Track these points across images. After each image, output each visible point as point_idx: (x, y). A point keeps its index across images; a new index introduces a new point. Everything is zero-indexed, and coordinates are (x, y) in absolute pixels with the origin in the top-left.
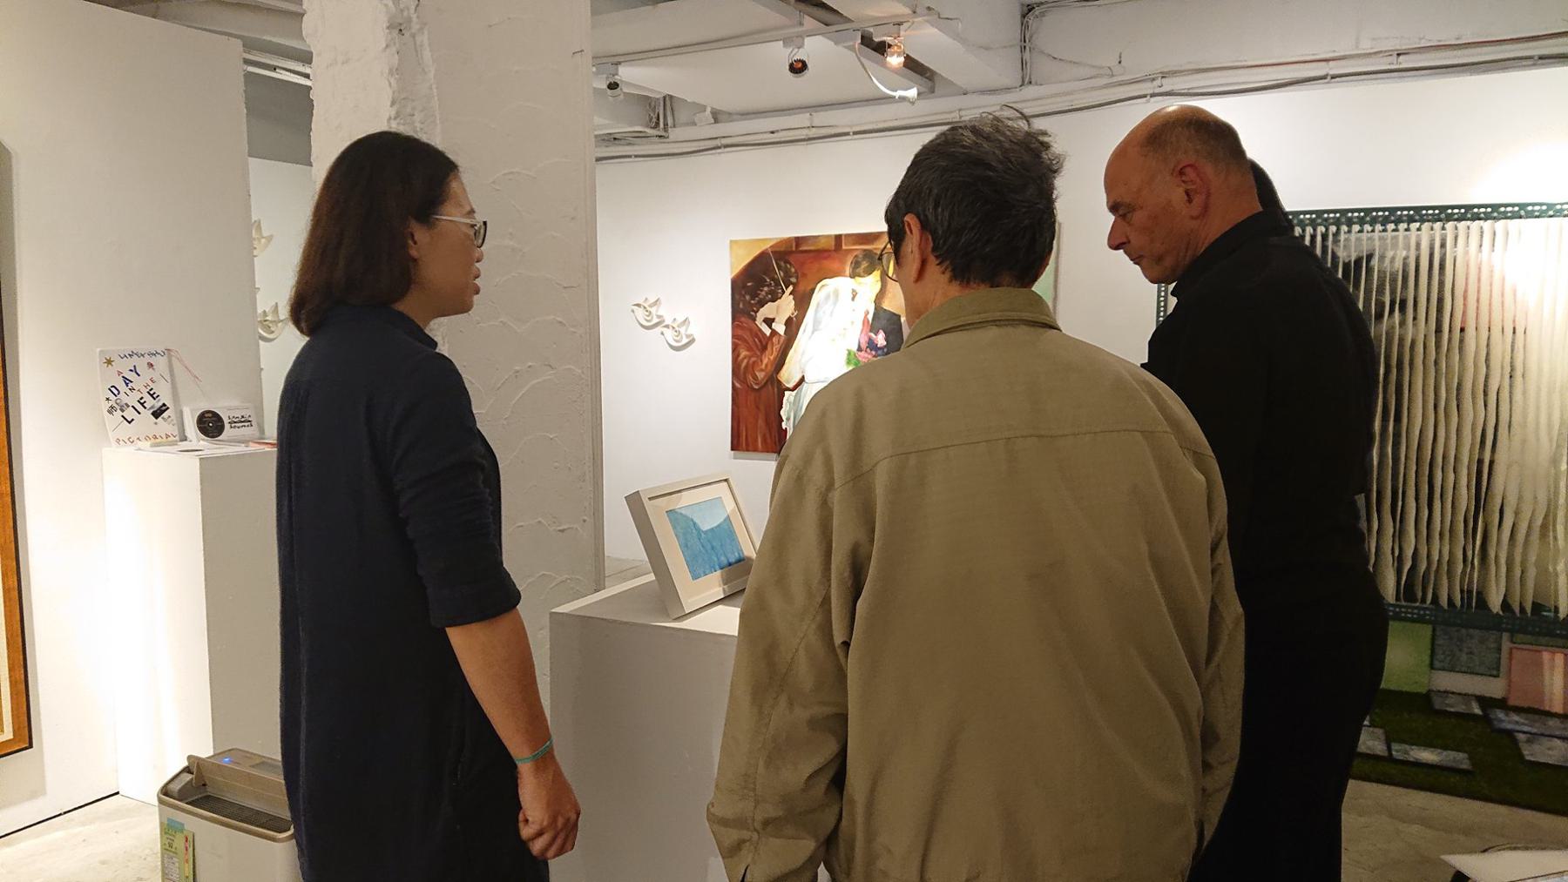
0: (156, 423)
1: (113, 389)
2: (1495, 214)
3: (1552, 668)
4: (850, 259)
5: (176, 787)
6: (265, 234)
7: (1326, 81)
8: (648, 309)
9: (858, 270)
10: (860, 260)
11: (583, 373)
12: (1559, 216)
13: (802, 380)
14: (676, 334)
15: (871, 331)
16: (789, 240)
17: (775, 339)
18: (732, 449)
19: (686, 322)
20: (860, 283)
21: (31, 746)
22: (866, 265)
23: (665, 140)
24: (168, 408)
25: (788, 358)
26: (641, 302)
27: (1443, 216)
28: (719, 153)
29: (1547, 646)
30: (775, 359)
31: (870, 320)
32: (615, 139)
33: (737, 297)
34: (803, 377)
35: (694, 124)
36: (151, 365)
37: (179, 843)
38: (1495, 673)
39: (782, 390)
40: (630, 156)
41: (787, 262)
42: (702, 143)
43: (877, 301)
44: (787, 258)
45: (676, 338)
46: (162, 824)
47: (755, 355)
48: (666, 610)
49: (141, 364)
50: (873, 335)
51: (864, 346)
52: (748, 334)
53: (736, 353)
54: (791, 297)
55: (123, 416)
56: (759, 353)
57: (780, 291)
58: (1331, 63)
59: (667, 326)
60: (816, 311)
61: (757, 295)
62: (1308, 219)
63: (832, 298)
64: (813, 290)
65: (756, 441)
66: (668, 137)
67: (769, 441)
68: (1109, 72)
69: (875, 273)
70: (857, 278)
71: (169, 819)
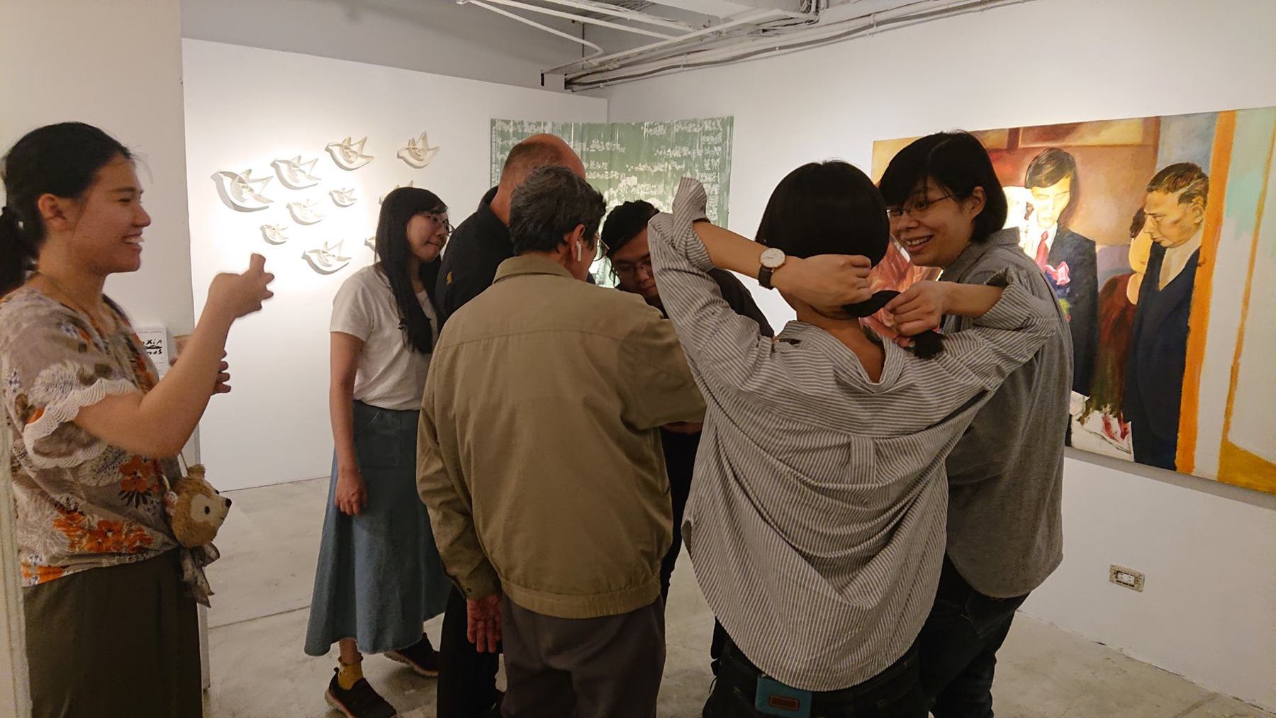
4: (1028, 160)
9: (1038, 177)
15: (1049, 262)
20: (1040, 195)
22: (1051, 169)
31: (1049, 247)
32: (764, 31)
40: (774, 49)
50: (1051, 268)
56: (894, 283)
66: (818, 21)
69: (1061, 181)
70: (1035, 188)
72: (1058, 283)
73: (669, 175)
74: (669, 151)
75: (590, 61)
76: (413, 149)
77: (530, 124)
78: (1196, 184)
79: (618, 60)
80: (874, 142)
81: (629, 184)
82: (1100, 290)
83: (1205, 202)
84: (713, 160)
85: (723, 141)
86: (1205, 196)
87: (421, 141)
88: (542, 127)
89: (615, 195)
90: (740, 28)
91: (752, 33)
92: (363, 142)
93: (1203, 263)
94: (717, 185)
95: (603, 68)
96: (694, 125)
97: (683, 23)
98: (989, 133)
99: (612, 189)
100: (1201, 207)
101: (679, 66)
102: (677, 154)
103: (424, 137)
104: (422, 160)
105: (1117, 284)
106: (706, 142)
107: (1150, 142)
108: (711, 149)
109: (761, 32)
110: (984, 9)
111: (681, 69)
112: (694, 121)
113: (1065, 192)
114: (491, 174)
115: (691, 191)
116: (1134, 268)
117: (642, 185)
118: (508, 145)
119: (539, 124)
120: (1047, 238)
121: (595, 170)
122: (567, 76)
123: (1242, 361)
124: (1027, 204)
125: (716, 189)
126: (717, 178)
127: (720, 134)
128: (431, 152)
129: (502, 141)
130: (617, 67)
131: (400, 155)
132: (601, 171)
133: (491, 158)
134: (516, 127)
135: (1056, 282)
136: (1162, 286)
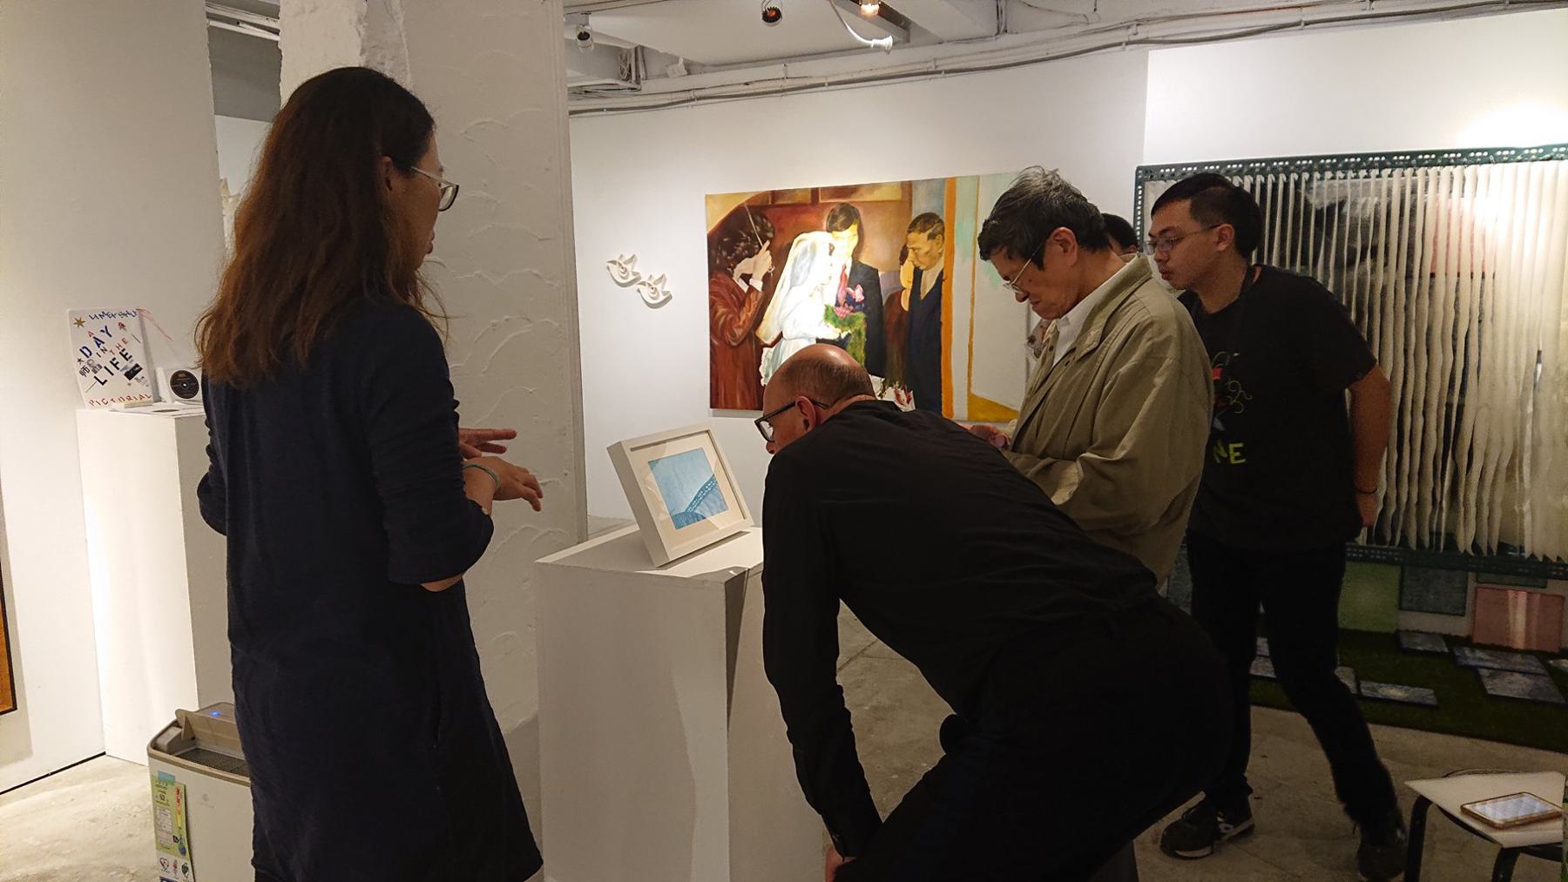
0: (129, 384)
1: (85, 350)
2: (1465, 160)
3: (1515, 607)
4: (826, 214)
5: (164, 742)
7: (1299, 27)
8: (624, 265)
9: (834, 225)
10: (837, 214)
11: (560, 326)
12: (1526, 161)
13: (781, 336)
14: (652, 291)
15: (849, 286)
16: (766, 194)
17: (752, 296)
18: (711, 407)
19: (662, 278)
21: (15, 708)
24: (141, 369)
25: (766, 313)
26: (616, 258)
27: (1414, 161)
28: (692, 106)
29: (1510, 584)
30: (753, 315)
32: (586, 92)
33: (713, 253)
35: (666, 76)
36: (122, 326)
37: (171, 796)
38: (1460, 611)
39: (760, 347)
40: (602, 110)
41: (763, 216)
42: (674, 95)
44: (763, 212)
45: (652, 295)
46: (152, 776)
47: (733, 312)
48: (651, 561)
49: (112, 325)
50: (850, 290)
51: (842, 301)
52: (725, 290)
53: (714, 308)
54: (768, 252)
55: (95, 377)
56: (735, 309)
57: (757, 246)
58: (1304, 9)
59: (643, 284)
60: (794, 266)
61: (734, 251)
62: (1282, 166)
63: (809, 255)
65: (735, 398)
67: (747, 397)
68: (1084, 20)
70: (834, 232)
71: (159, 772)
78: (937, 227)
80: (706, 196)
82: (884, 302)
83: (943, 238)
86: (943, 235)
93: (947, 277)
100: (941, 242)
105: (895, 297)
107: (907, 199)
116: (904, 286)
123: (974, 340)
136: (922, 297)
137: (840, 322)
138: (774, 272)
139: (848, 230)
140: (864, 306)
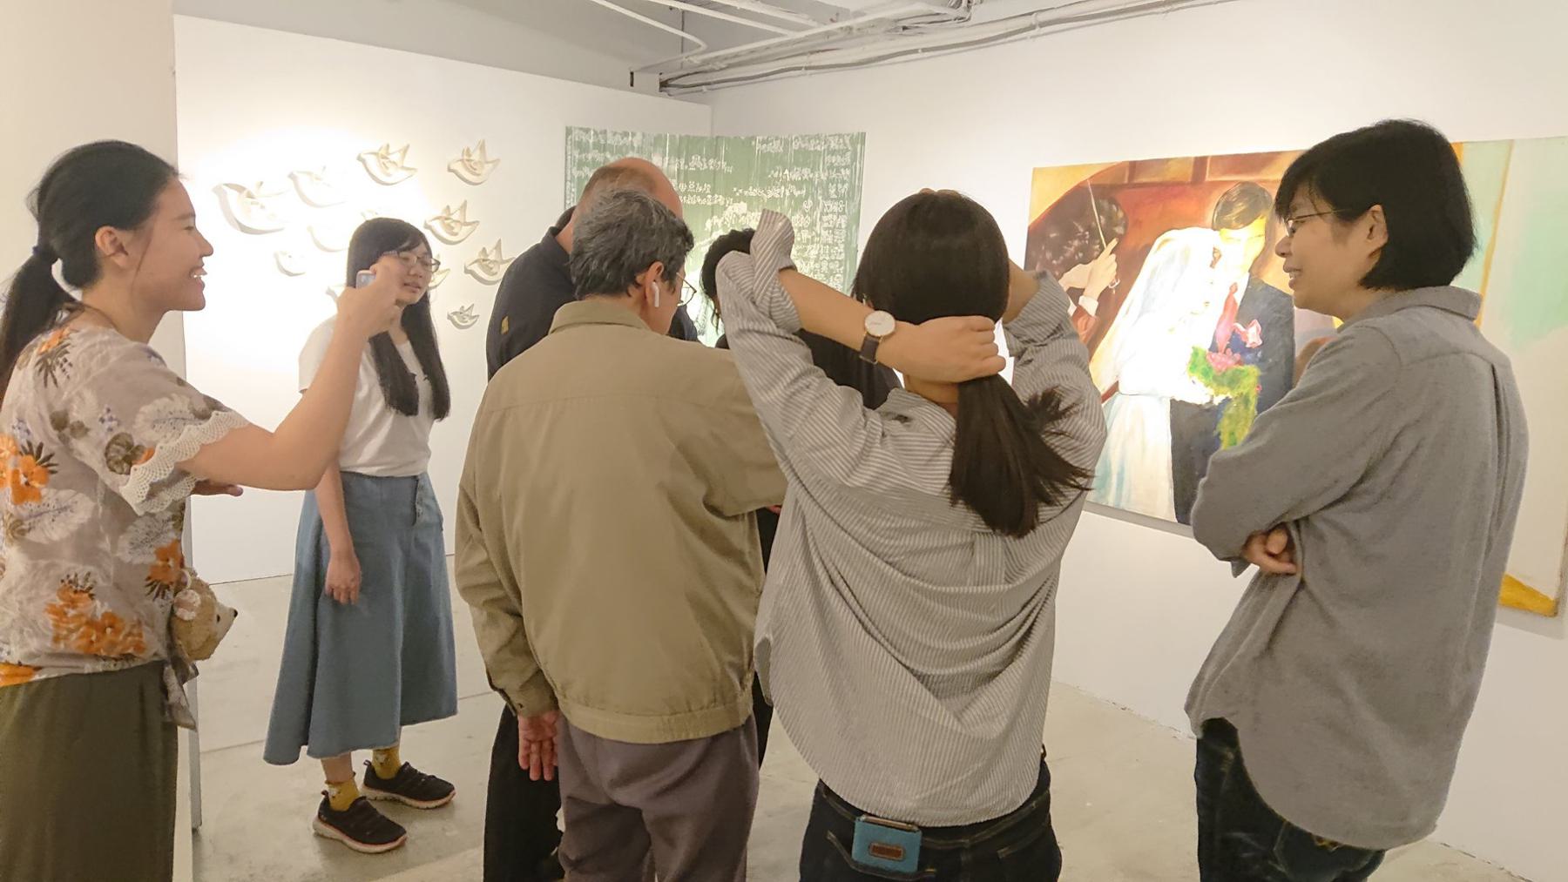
4: (1216, 197)
6: (491, 156)
9: (1227, 217)
13: (1114, 389)
15: (1238, 319)
16: (1118, 168)
17: (1081, 322)
22: (1243, 208)
23: (969, 23)
32: (905, 28)
34: (1117, 383)
40: (915, 51)
41: (1112, 201)
43: (1254, 271)
50: (1239, 326)
51: (1223, 343)
54: (1114, 256)
57: (1098, 246)
64: (1148, 248)
66: (969, 19)
70: (1224, 231)
72: (1248, 346)
73: (786, 202)
74: (787, 172)
75: (691, 59)
76: (468, 160)
77: (615, 134)
79: (726, 59)
80: (1035, 169)
81: (737, 211)
82: (1297, 354)
84: (840, 186)
85: (852, 164)
87: (478, 152)
88: (630, 138)
89: (720, 225)
90: (874, 24)
91: (889, 31)
92: (405, 150)
94: (845, 216)
95: (706, 68)
96: (818, 142)
97: (806, 16)
98: (1170, 163)
99: (715, 217)
101: (800, 69)
102: (796, 177)
103: (482, 147)
104: (478, 175)
106: (832, 164)
108: (838, 171)
109: (901, 30)
110: (1167, 12)
111: (803, 71)
112: (817, 137)
113: (1259, 236)
114: (565, 196)
115: (777, 230)
117: (753, 214)
118: (587, 159)
119: (626, 134)
120: (1236, 290)
121: (694, 193)
122: (662, 77)
124: (1214, 249)
125: (843, 221)
126: (844, 208)
127: (849, 153)
128: (491, 165)
129: (579, 154)
130: (724, 66)
131: (452, 168)
132: (703, 195)
133: (566, 176)
134: (597, 135)
135: (1245, 344)
137: (1215, 378)
138: (1116, 288)
139: (1247, 227)
140: (1261, 356)
